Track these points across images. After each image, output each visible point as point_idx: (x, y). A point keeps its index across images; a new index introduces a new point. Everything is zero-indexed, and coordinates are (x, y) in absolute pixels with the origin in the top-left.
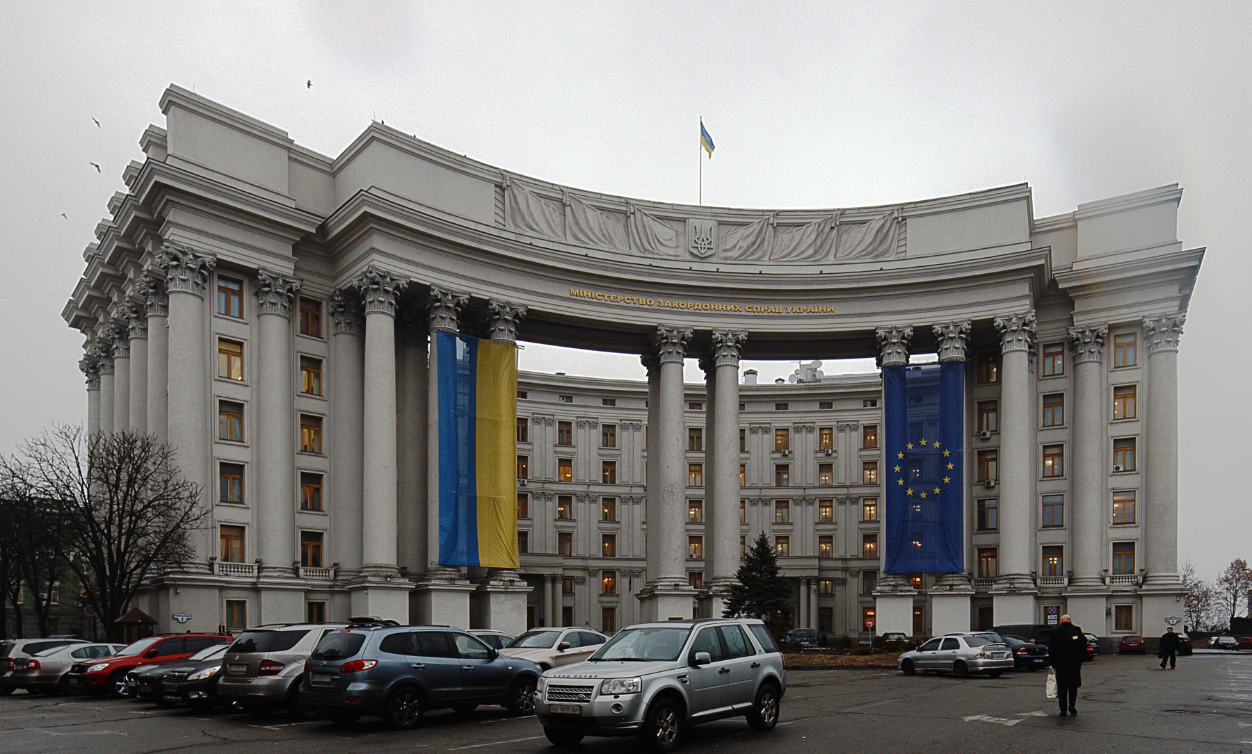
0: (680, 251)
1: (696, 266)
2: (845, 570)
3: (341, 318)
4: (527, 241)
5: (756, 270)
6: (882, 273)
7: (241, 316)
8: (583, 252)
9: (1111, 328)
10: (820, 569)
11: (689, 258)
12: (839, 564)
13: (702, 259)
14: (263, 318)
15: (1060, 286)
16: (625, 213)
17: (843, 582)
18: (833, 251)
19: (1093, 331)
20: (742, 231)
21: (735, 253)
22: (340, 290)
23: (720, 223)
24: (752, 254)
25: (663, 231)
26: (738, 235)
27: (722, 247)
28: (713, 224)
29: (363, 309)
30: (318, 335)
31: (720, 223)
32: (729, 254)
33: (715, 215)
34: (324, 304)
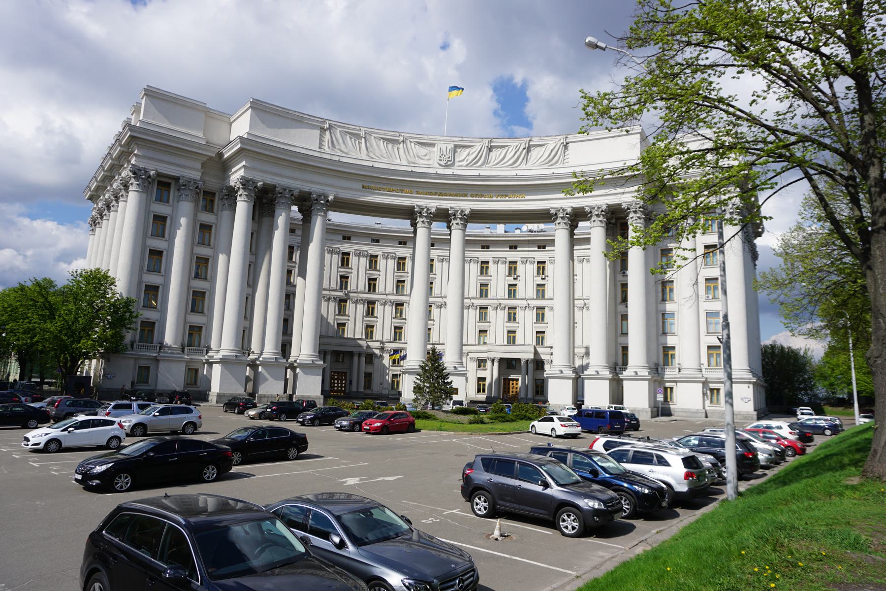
0: (431, 162)
1: (441, 171)
3: (226, 202)
4: (337, 158)
5: (476, 173)
6: (553, 176)
7: (168, 202)
8: (370, 164)
10: (536, 353)
11: (438, 166)
13: (446, 166)
14: (181, 203)
16: (398, 141)
18: (525, 161)
20: (468, 150)
21: (465, 163)
23: (456, 146)
24: (476, 163)
25: (422, 151)
26: (466, 153)
27: (457, 160)
29: (236, 198)
30: (212, 212)
31: (456, 146)
32: (461, 164)
33: (453, 141)
34: (217, 194)
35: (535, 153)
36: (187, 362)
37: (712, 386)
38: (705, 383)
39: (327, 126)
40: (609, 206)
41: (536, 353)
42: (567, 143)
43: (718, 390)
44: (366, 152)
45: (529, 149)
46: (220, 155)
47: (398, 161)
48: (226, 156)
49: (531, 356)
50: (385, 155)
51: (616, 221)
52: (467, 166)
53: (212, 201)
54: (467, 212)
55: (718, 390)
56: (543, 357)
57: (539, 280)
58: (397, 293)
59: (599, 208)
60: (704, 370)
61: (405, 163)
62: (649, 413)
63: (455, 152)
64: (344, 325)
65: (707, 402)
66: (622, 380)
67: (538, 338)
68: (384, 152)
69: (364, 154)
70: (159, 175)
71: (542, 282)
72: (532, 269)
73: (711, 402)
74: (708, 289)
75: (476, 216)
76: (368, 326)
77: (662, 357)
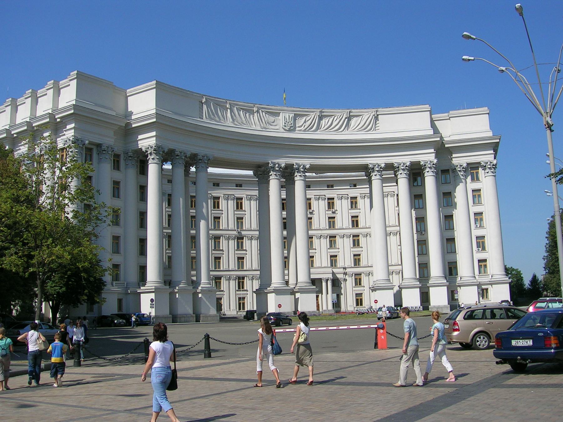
0: (277, 127)
2: (345, 274)
9: (468, 164)
10: (333, 273)
11: (283, 131)
12: (342, 270)
13: (289, 131)
15: (446, 146)
17: (345, 280)
19: (461, 166)
20: (304, 118)
22: (132, 150)
25: (272, 119)
27: (297, 126)
28: (292, 115)
33: (293, 111)
35: (354, 121)
36: (119, 293)
37: (484, 287)
38: (479, 285)
39: (204, 100)
40: (412, 164)
41: (333, 273)
42: (378, 115)
43: (487, 289)
44: (231, 120)
45: (349, 118)
46: (128, 124)
47: (254, 127)
48: (133, 126)
49: (330, 276)
50: (245, 122)
51: (416, 173)
52: (305, 130)
53: (118, 161)
54: (308, 166)
55: (487, 289)
56: (339, 276)
57: (330, 214)
58: (215, 229)
59: (404, 164)
60: (477, 277)
61: (259, 128)
62: (449, 308)
63: (295, 120)
64: (220, 258)
65: (481, 298)
66: (429, 287)
67: (331, 261)
68: (244, 119)
69: (229, 122)
70: (90, 143)
71: (333, 215)
72: (323, 204)
73: (483, 298)
74: (476, 220)
75: (313, 168)
76: (239, 258)
77: (451, 270)
